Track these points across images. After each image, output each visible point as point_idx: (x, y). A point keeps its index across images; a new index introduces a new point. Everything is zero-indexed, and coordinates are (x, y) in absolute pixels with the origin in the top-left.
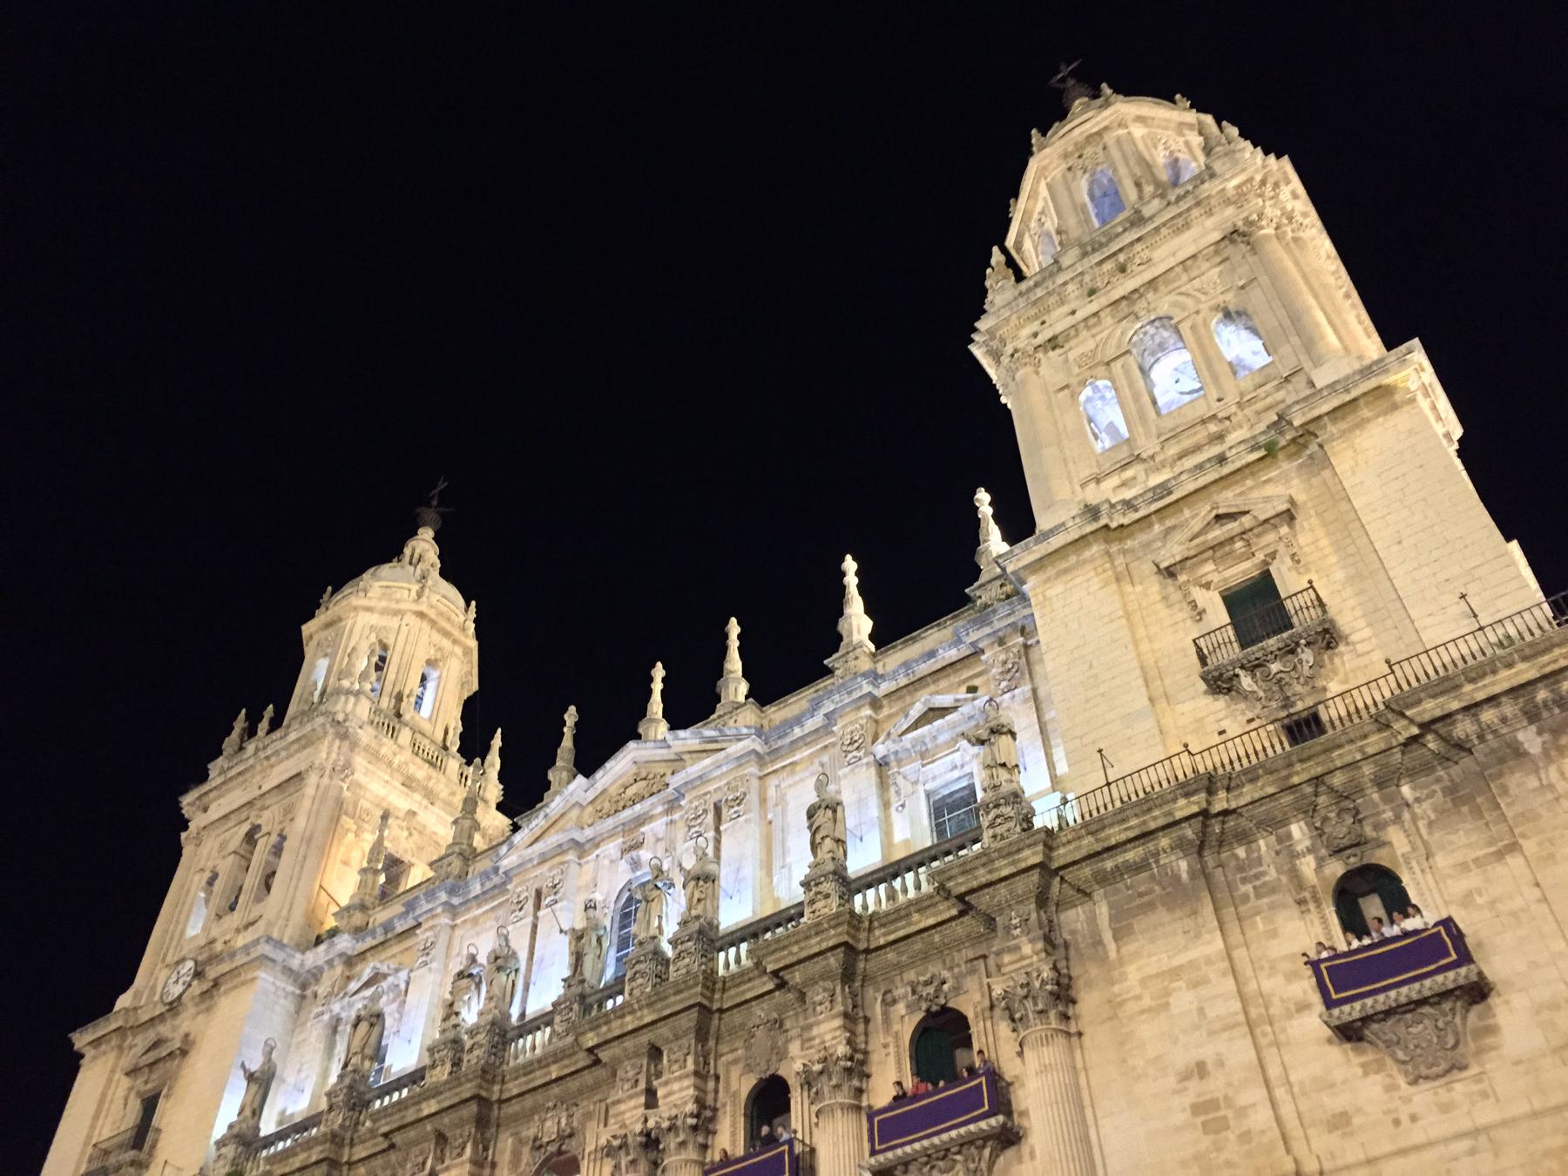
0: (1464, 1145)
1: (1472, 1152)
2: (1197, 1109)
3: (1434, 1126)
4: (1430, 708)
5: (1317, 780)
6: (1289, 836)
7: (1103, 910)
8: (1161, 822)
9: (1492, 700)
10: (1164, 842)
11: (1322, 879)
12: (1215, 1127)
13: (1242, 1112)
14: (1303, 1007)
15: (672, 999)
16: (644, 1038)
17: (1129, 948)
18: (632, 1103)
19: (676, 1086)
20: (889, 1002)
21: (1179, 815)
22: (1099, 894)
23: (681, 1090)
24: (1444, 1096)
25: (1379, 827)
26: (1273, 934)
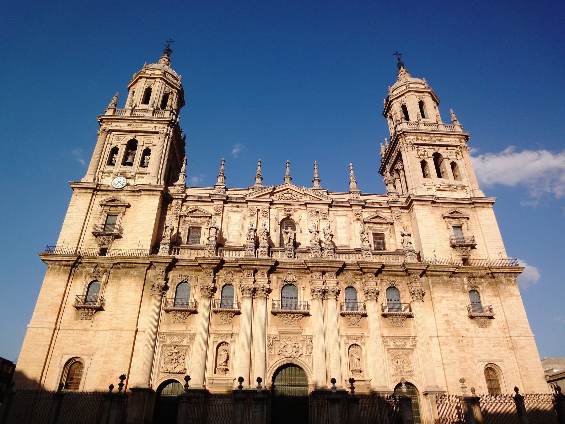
0: (485, 338)
1: (486, 340)
2: (446, 321)
3: (481, 335)
4: (494, 270)
5: (472, 273)
6: (463, 280)
7: (430, 281)
8: (447, 270)
9: (502, 273)
10: (445, 273)
11: (468, 289)
12: (450, 325)
13: (454, 324)
14: (463, 310)
15: (335, 264)
16: (323, 269)
17: (435, 289)
18: (319, 282)
19: (332, 282)
20: (382, 281)
21: (450, 270)
22: (429, 277)
23: (333, 283)
24: (484, 331)
25: (478, 284)
26: (459, 296)
